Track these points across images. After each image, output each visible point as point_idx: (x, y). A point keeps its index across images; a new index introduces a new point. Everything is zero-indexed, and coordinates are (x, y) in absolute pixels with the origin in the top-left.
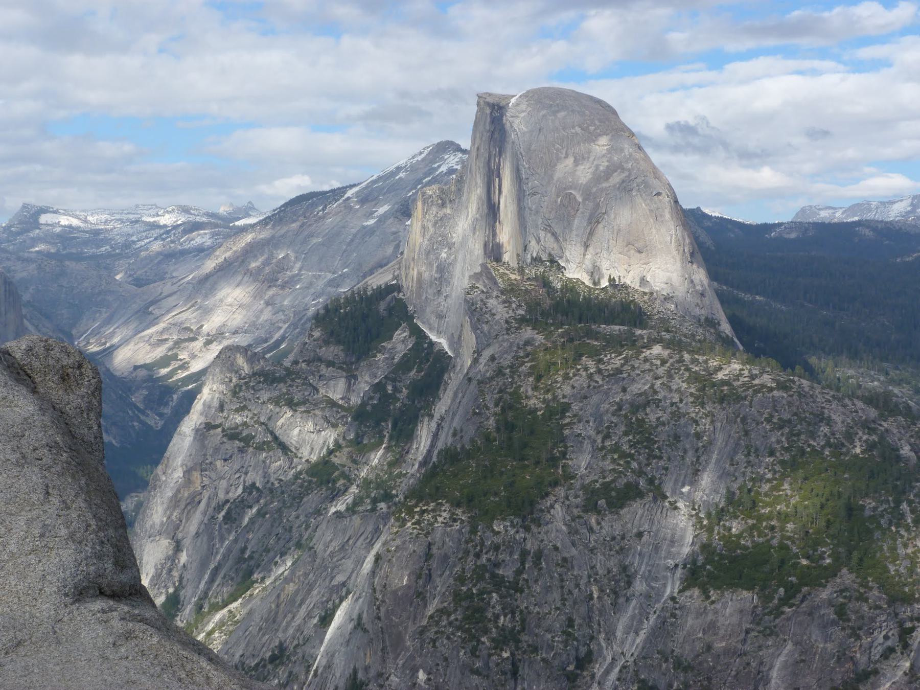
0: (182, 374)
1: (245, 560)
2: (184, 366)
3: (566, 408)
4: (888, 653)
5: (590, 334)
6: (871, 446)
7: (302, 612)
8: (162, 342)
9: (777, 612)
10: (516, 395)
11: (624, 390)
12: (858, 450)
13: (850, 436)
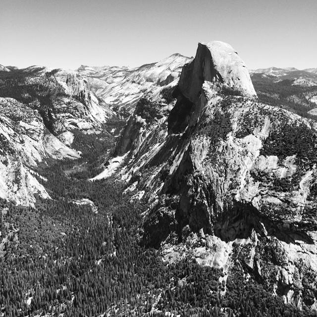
0: (120, 103)
1: (148, 145)
2: (121, 102)
4: (307, 170)
6: (301, 125)
7: (163, 156)
8: (115, 96)
9: (282, 161)
11: (243, 111)
12: (298, 125)
13: (296, 124)
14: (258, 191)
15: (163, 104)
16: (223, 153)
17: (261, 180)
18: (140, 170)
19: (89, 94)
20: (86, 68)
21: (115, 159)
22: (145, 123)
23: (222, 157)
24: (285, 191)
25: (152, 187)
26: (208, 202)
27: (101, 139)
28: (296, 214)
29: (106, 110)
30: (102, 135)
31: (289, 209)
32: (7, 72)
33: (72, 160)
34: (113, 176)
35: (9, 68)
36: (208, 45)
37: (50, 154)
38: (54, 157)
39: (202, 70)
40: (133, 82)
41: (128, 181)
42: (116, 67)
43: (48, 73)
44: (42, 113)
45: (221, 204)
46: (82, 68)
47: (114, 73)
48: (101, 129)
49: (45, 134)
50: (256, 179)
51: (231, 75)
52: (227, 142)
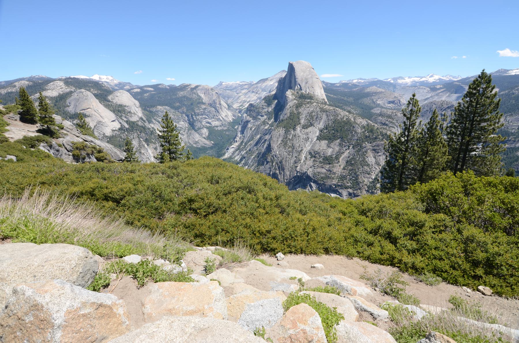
3: (300, 113)
5: (304, 101)
6: (347, 119)
10: (293, 111)
13: (343, 118)
14: (312, 164)
15: (265, 107)
16: (292, 140)
17: (315, 157)
18: (246, 153)
19: (220, 102)
20: (223, 84)
21: (232, 146)
22: (252, 121)
23: (291, 142)
24: (329, 164)
25: (251, 164)
26: (280, 173)
27: (227, 133)
28: (334, 179)
29: (233, 113)
30: (228, 130)
31: (330, 176)
32: (167, 89)
33: (206, 147)
34: (230, 158)
35: (168, 86)
36: (294, 64)
37: (192, 143)
38: (194, 145)
39: (290, 82)
40: (253, 92)
41: (238, 160)
42: (244, 82)
43: (192, 88)
44: (188, 116)
45: (288, 173)
46: (221, 84)
47: (241, 86)
48: (227, 126)
49: (188, 130)
50: (312, 156)
51: (308, 85)
52: (296, 132)
